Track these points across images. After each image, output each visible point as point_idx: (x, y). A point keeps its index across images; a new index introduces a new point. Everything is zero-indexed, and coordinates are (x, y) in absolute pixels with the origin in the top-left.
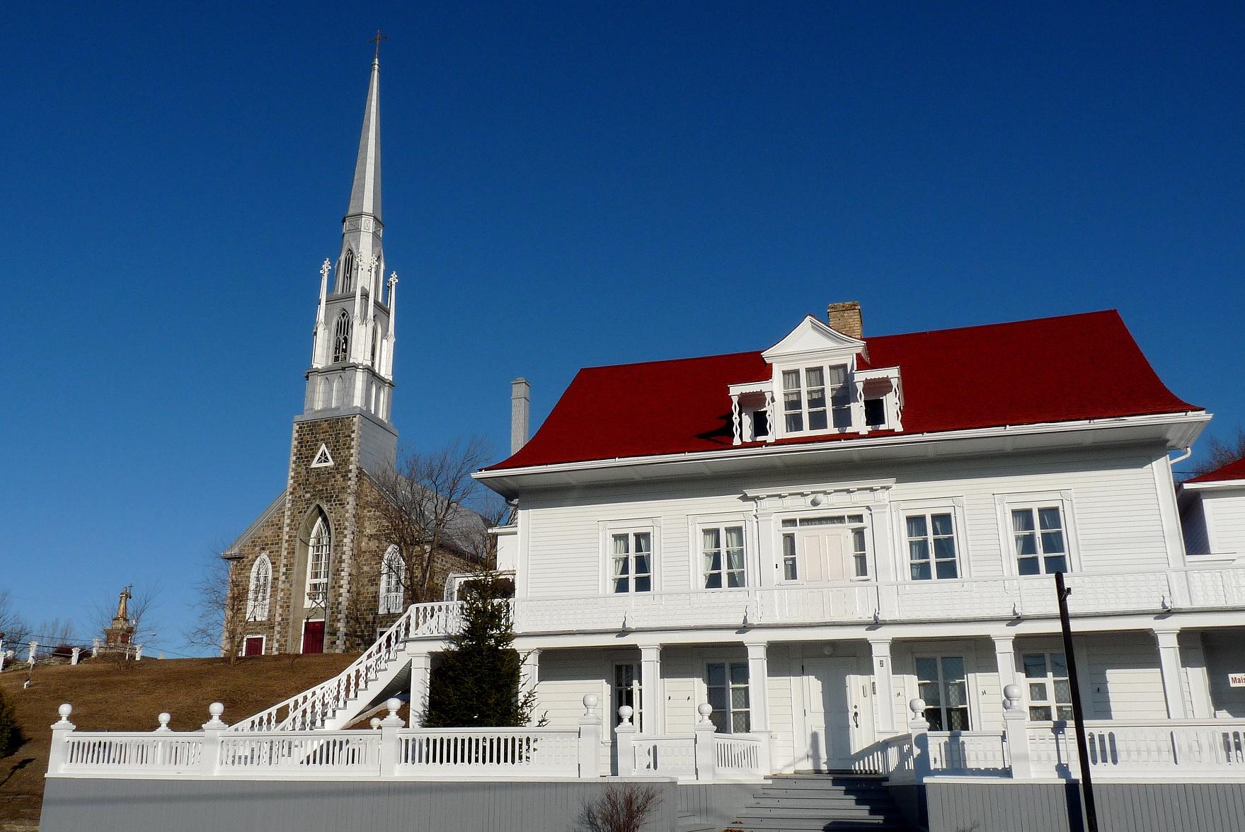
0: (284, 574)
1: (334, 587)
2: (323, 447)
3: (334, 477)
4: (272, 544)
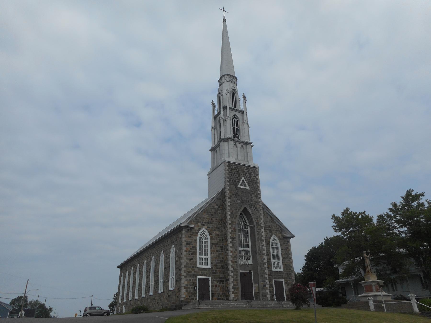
0: (231, 242)
1: (260, 254)
2: (243, 178)
3: (251, 195)
4: (209, 223)
